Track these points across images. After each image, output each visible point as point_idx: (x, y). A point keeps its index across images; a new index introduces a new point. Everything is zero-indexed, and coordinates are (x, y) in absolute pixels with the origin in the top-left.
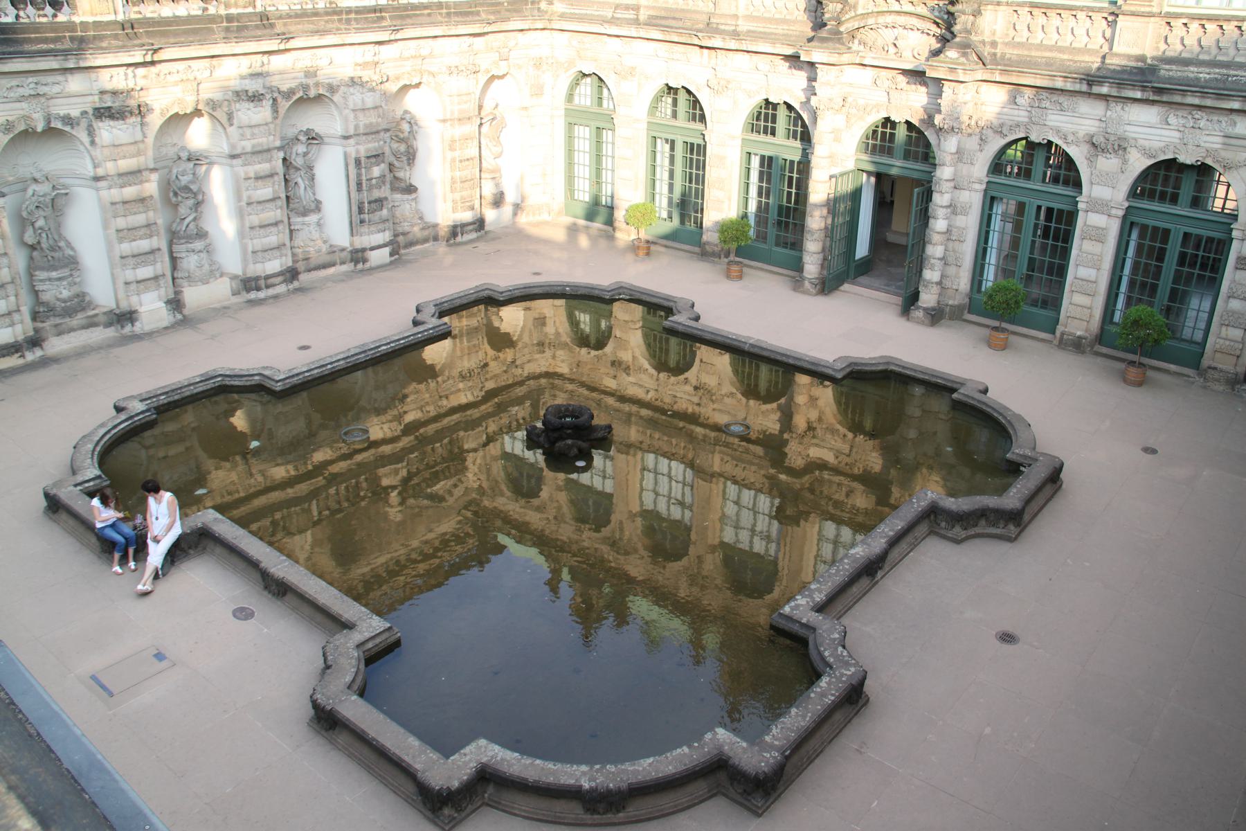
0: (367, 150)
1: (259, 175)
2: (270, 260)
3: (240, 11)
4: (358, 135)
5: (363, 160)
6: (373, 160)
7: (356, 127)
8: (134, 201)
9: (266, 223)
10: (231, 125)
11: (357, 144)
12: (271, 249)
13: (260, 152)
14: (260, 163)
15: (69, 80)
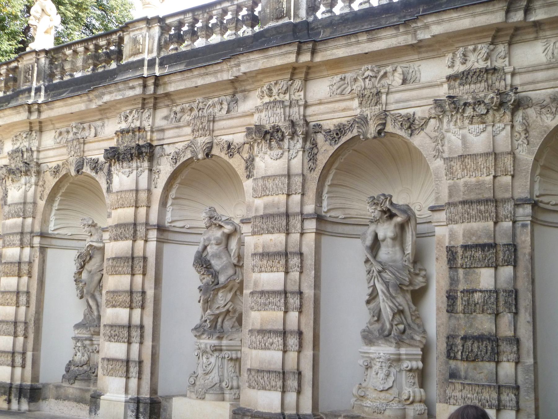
0: (468, 234)
1: (267, 250)
2: (264, 388)
3: (272, 24)
4: (454, 204)
5: (460, 252)
6: (479, 254)
7: (452, 190)
8: (121, 258)
9: (269, 327)
10: (248, 177)
11: (451, 220)
12: (269, 372)
13: (272, 216)
14: (269, 232)
15: (105, 125)
